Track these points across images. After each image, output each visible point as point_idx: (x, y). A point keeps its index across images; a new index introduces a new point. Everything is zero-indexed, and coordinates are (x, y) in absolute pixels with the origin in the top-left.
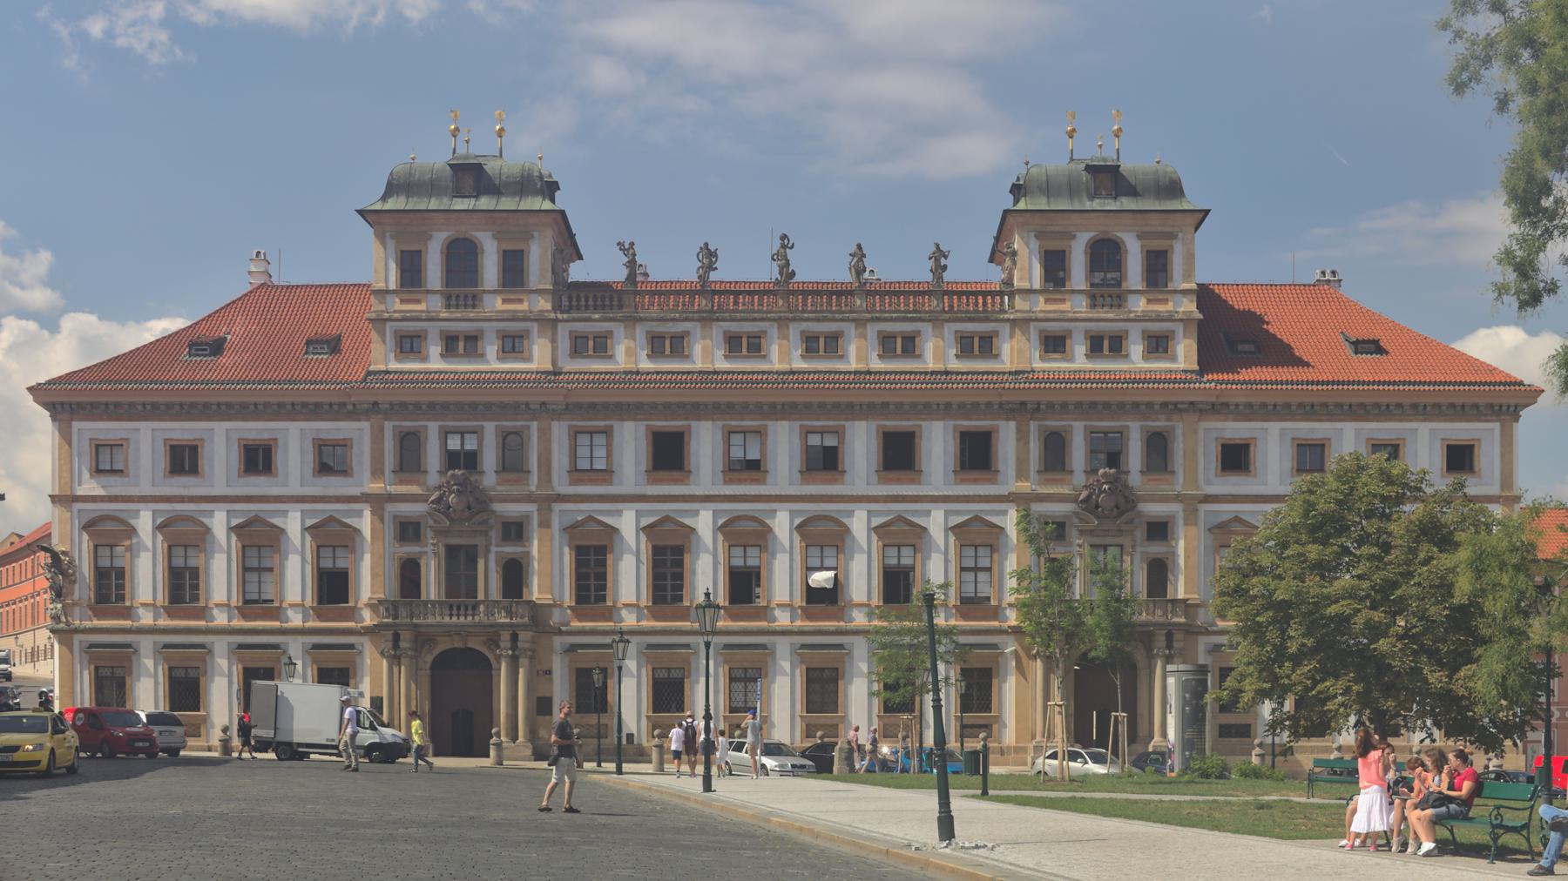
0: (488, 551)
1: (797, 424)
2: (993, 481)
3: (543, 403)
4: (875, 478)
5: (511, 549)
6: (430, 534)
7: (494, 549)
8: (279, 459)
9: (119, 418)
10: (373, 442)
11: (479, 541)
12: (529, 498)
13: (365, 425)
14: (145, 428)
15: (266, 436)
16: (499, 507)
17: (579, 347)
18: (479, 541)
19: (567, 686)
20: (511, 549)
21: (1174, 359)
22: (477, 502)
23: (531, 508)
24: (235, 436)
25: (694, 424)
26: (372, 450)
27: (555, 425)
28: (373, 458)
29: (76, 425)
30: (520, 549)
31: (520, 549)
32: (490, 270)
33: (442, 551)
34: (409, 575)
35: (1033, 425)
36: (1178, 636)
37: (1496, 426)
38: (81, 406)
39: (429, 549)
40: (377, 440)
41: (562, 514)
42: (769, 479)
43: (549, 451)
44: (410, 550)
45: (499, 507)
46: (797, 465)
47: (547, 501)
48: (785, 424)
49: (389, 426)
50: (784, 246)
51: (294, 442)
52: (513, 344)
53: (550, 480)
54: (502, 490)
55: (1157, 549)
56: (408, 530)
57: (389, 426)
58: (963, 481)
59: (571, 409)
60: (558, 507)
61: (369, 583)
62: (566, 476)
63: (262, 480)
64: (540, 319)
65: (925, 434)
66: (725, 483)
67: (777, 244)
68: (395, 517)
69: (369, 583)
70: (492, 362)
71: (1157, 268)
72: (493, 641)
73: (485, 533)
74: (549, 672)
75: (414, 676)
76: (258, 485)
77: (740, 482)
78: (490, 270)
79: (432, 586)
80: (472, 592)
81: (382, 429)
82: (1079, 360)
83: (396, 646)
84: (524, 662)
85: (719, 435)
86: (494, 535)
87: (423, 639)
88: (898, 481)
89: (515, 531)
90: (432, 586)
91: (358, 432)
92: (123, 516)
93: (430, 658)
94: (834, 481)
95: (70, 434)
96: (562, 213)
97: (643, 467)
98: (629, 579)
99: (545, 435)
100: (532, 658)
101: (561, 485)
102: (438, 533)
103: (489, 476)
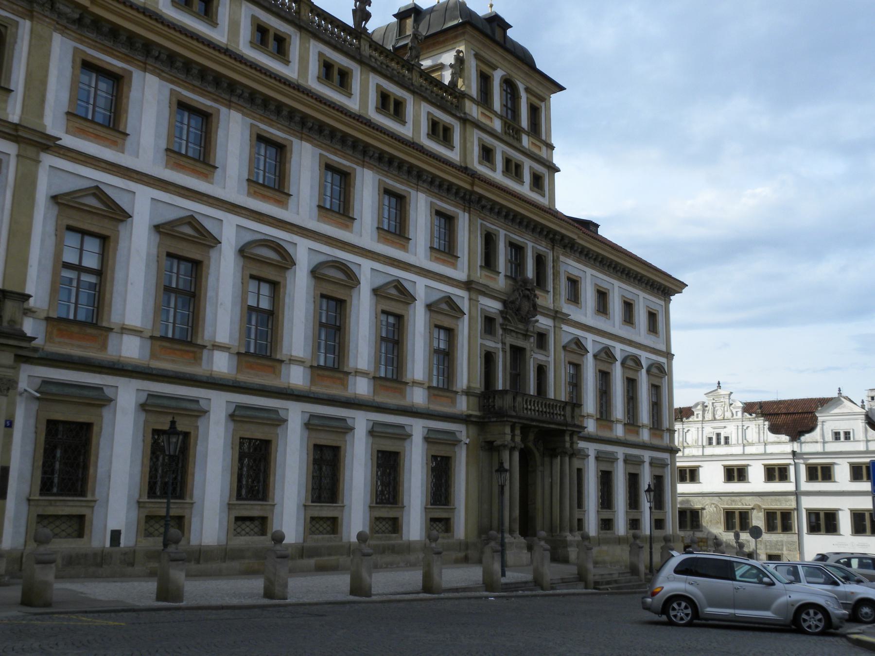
2: (454, 266)
19: (30, 448)
25: (224, 110)
35: (480, 221)
36: (575, 438)
37: (663, 303)
41: (52, 176)
42: (292, 202)
43: (45, 69)
46: (315, 202)
53: (41, 116)
55: (540, 357)
58: (437, 260)
60: (48, 160)
62: (62, 120)
66: (249, 194)
77: (265, 198)
82: (498, 176)
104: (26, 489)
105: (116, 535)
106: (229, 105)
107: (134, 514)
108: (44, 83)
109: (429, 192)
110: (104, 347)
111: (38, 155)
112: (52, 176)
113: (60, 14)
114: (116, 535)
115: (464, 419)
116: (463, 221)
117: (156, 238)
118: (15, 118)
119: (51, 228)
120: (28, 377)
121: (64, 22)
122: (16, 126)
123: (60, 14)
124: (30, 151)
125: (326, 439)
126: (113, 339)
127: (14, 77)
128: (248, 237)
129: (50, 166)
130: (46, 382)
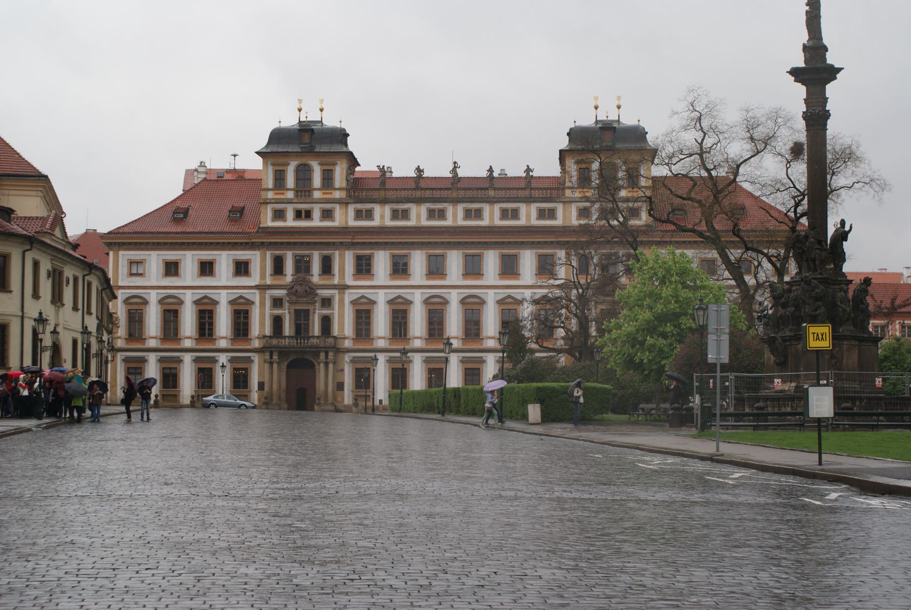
1: (461, 252)
3: (341, 243)
4: (498, 277)
5: (326, 312)
7: (317, 311)
8: (217, 268)
9: (142, 250)
11: (311, 308)
12: (334, 287)
13: (258, 253)
14: (154, 254)
15: (210, 258)
16: (319, 291)
17: (359, 215)
18: (311, 308)
19: (351, 376)
20: (326, 312)
21: (640, 219)
22: (310, 291)
23: (336, 292)
24: (196, 258)
25: (412, 252)
27: (347, 252)
29: (121, 253)
30: (329, 312)
31: (329, 312)
32: (317, 181)
33: (292, 311)
34: (277, 322)
38: (124, 244)
39: (287, 311)
40: (263, 260)
41: (349, 296)
44: (277, 312)
45: (319, 291)
46: (461, 272)
47: (343, 288)
48: (456, 251)
49: (268, 254)
50: (455, 167)
51: (224, 260)
52: (327, 214)
53: (344, 279)
54: (321, 283)
56: (277, 302)
59: (352, 245)
61: (259, 325)
62: (352, 278)
63: (208, 278)
64: (340, 202)
65: (522, 257)
67: (451, 167)
69: (259, 325)
70: (316, 222)
71: (633, 179)
72: (316, 354)
73: (314, 303)
74: (343, 370)
75: (280, 370)
76: (207, 281)
77: (434, 279)
78: (317, 181)
79: (288, 329)
80: (307, 329)
83: (271, 358)
84: (331, 366)
85: (424, 257)
86: (318, 305)
87: (283, 353)
88: (509, 279)
89: (327, 302)
90: (288, 329)
91: (255, 257)
92: (143, 295)
93: (286, 363)
94: (478, 279)
95: (118, 257)
96: (351, 153)
97: (388, 273)
98: (381, 324)
99: (342, 258)
100: (334, 363)
101: (349, 281)
102: (290, 303)
103: (316, 277)
104: (351, 388)
105: (381, 401)
106: (415, 249)
107: (387, 395)
109: (530, 249)
110: (372, 344)
112: (349, 296)
114: (381, 401)
115: (559, 351)
116: (561, 254)
117: (388, 306)
118: (336, 282)
119: (351, 311)
120: (347, 357)
122: (335, 285)
125: (470, 366)
126: (374, 342)
128: (427, 296)
130: (354, 357)
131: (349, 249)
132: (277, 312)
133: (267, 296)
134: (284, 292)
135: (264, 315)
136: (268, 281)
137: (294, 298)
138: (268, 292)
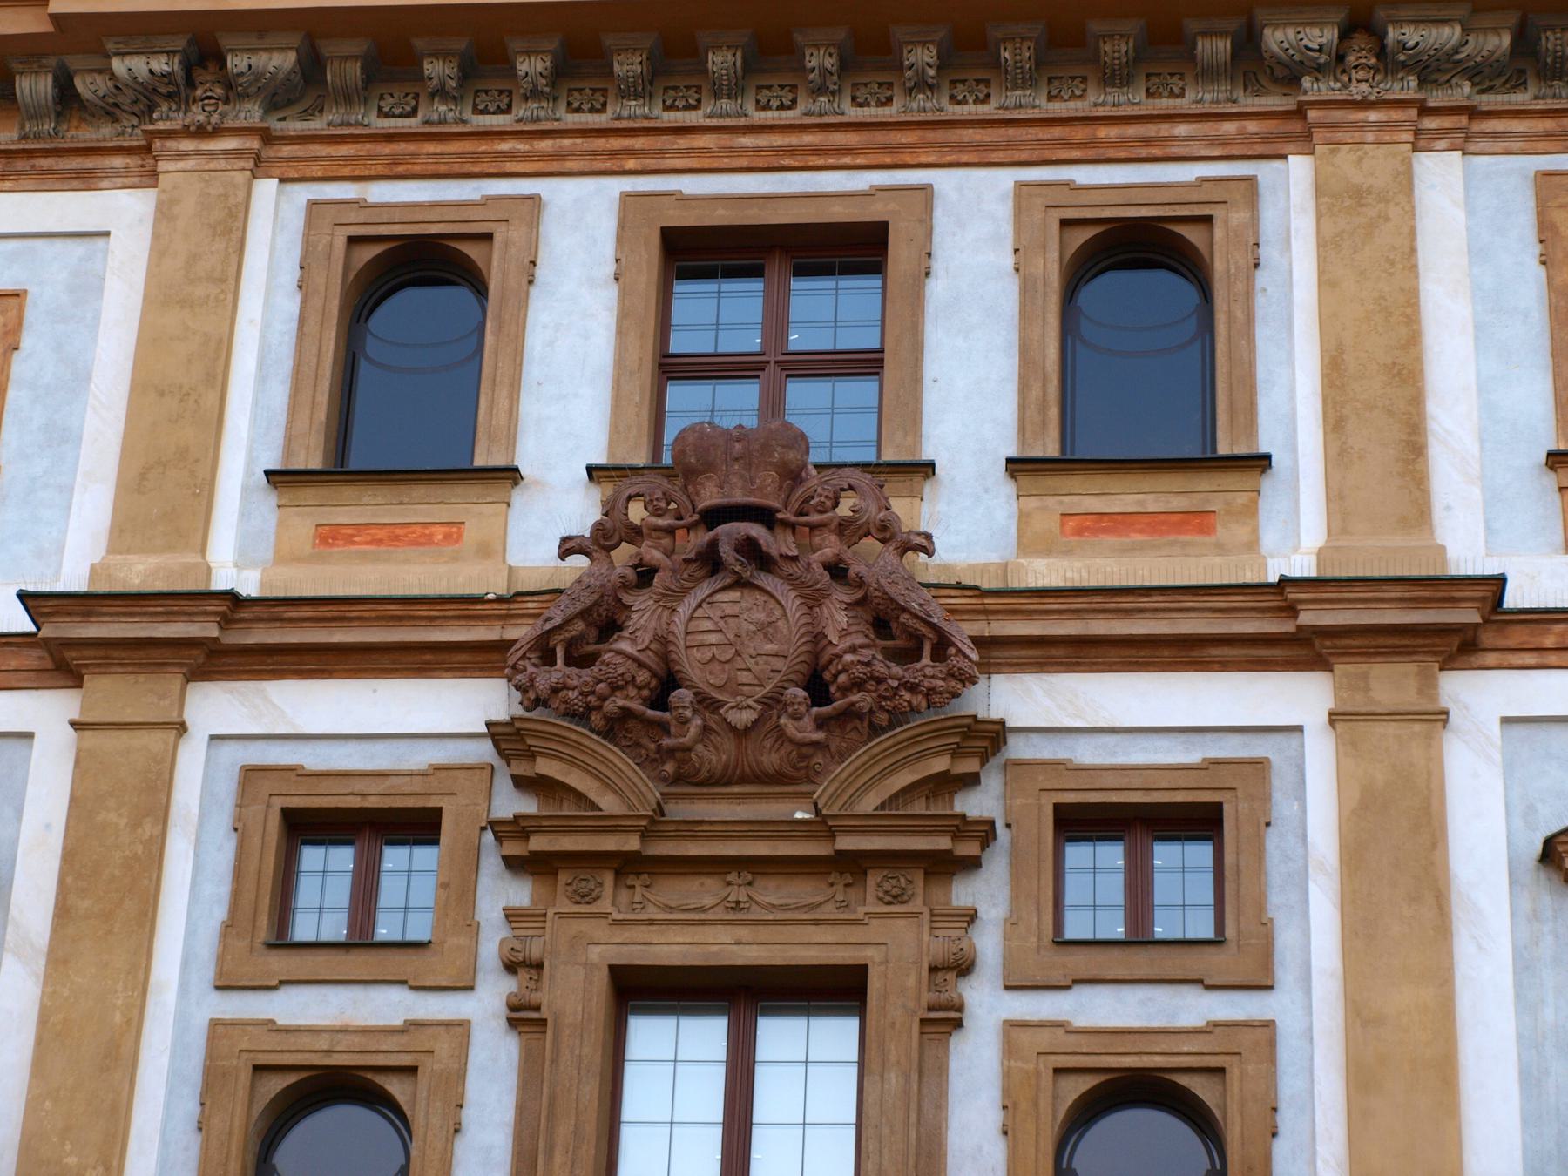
0: (945, 1020)
6: (497, 893)
7: (988, 1004)
10: (163, 296)
11: (889, 942)
13: (123, 211)
23: (1296, 699)
26: (149, 342)
28: (148, 387)
30: (1192, 1009)
31: (1192, 1009)
33: (575, 994)
39: (485, 1005)
40: (189, 298)
53: (1416, 508)
57: (277, 225)
60: (1481, 697)
68: (251, 775)
81: (231, 227)
108: (1406, 375)
111: (1428, 686)
113: (1431, 69)
121: (1463, 92)
123: (1431, 69)
124: (1390, 682)
127: (1268, 405)
129: (1506, 721)
131: (1467, 129)
132: (326, 1012)
133: (191, 763)
134: (461, 707)
135: (118, 1058)
136: (240, 550)
137: (614, 785)
138: (219, 707)
